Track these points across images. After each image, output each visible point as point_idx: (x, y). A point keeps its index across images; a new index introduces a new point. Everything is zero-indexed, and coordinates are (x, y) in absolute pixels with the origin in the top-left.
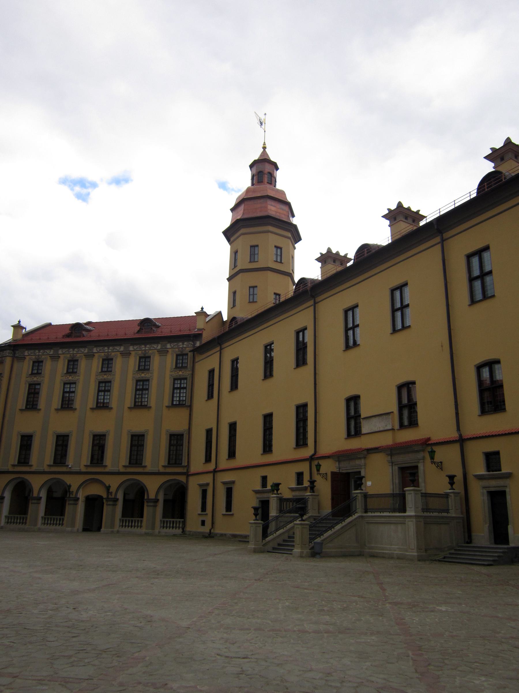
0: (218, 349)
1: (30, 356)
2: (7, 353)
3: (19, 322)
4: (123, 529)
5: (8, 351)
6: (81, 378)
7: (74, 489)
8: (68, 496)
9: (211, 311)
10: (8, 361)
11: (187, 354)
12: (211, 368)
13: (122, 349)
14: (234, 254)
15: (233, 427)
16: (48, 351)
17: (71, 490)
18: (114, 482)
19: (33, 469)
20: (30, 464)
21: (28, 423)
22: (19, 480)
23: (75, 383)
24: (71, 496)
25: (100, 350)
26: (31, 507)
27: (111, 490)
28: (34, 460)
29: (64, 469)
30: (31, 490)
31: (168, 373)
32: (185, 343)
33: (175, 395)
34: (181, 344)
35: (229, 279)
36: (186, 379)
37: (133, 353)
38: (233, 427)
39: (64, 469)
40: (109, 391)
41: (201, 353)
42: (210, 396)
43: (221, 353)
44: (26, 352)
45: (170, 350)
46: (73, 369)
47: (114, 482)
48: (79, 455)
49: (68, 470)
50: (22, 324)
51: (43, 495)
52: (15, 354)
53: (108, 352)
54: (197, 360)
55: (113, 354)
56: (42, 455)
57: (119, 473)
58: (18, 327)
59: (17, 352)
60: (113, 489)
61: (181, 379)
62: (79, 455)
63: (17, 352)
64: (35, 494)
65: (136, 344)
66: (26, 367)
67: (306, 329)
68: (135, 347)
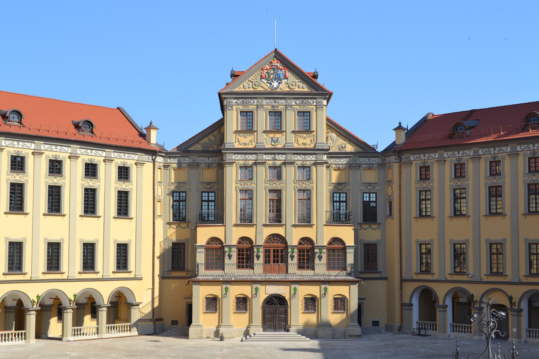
1: (416, 160)
2: (393, 158)
3: (400, 124)
4: (531, 340)
5: (394, 157)
6: (469, 182)
7: (477, 298)
8: (472, 305)
10: (396, 166)
13: (509, 149)
16: (433, 155)
17: (475, 299)
18: (517, 292)
19: (435, 278)
20: (432, 272)
21: (423, 231)
22: (423, 288)
23: (465, 189)
24: (476, 306)
25: (486, 152)
26: (439, 315)
27: (513, 301)
28: (435, 268)
29: (464, 278)
30: (437, 297)
37: (521, 154)
39: (464, 278)
40: (500, 196)
44: (412, 157)
46: (461, 172)
47: (517, 292)
48: (477, 263)
49: (469, 279)
50: (404, 125)
51: (449, 302)
52: (401, 159)
53: (495, 153)
55: (500, 155)
56: (442, 263)
57: (521, 283)
58: (400, 128)
59: (403, 157)
60: (516, 300)
62: (477, 263)
63: (403, 157)
64: (441, 303)
65: (524, 144)
66: (414, 172)
68: (523, 147)
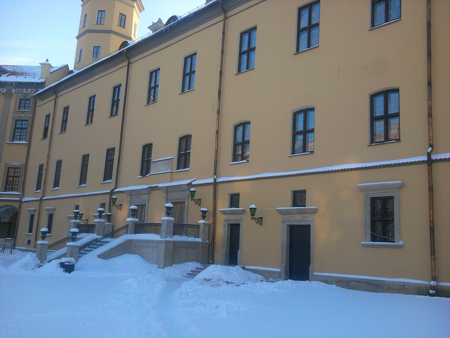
0: (54, 97)
9: (56, 64)
11: (30, 100)
12: (47, 113)
14: (85, 17)
15: (59, 163)
31: (11, 114)
32: (29, 90)
33: (16, 134)
34: (25, 90)
35: (78, 38)
36: (27, 121)
38: (59, 163)
41: (42, 100)
42: (45, 136)
43: (55, 101)
45: (14, 95)
54: (38, 105)
61: (22, 121)
67: (121, 85)
